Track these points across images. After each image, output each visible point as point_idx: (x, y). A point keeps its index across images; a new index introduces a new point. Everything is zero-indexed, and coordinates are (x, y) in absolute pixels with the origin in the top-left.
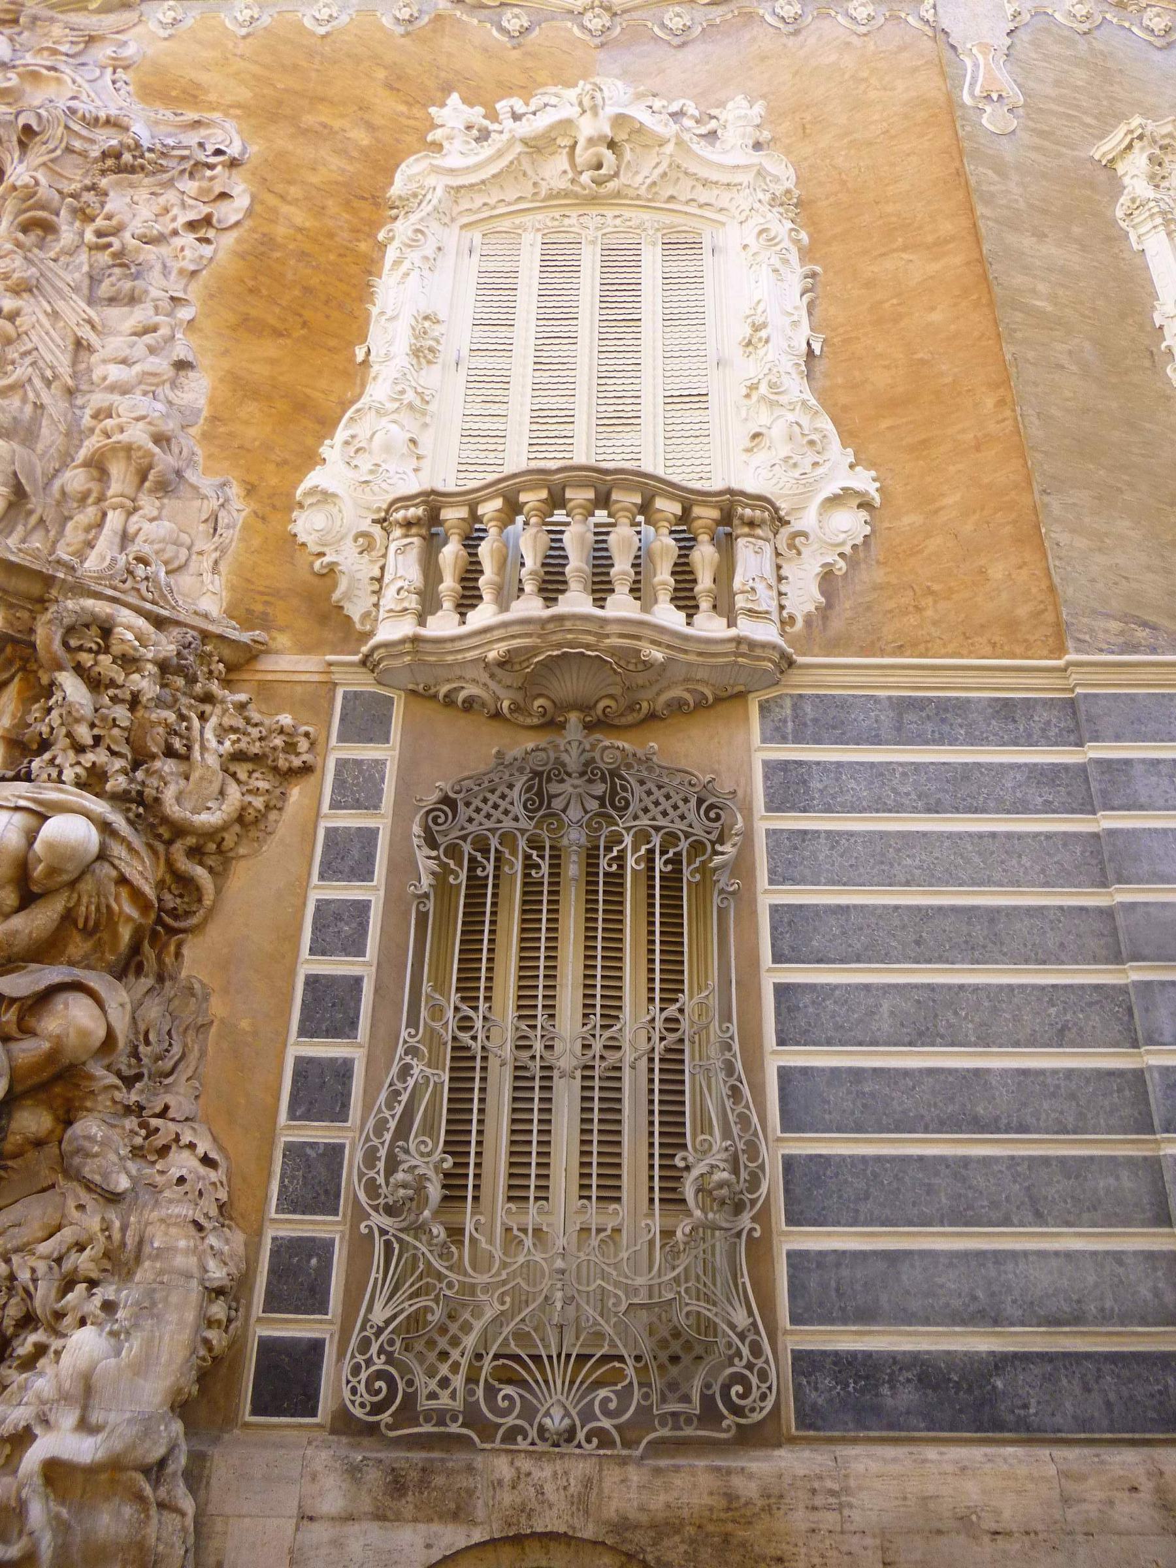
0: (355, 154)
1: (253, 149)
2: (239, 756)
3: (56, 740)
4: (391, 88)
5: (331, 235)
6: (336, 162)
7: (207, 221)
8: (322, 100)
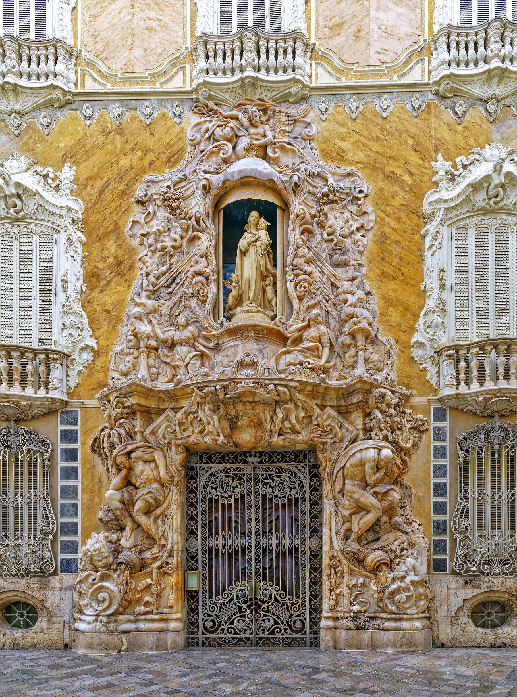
0: (407, 189)
1: (371, 187)
2: (412, 428)
4: (416, 151)
5: (405, 232)
6: (402, 194)
7: (362, 227)
8: (391, 158)
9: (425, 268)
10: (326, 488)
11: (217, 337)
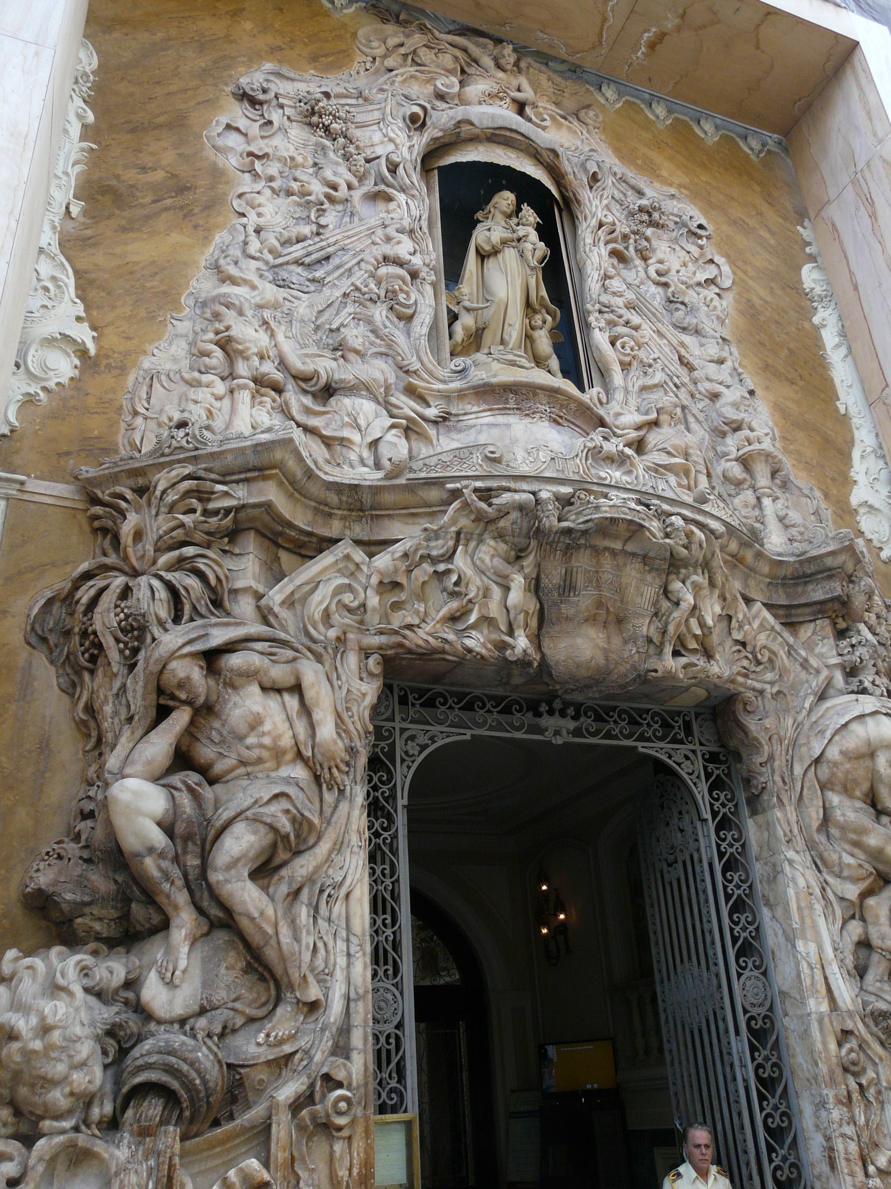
3: (863, 668)
8: (732, 198)
9: (837, 381)
10: (783, 817)
11: (447, 397)
